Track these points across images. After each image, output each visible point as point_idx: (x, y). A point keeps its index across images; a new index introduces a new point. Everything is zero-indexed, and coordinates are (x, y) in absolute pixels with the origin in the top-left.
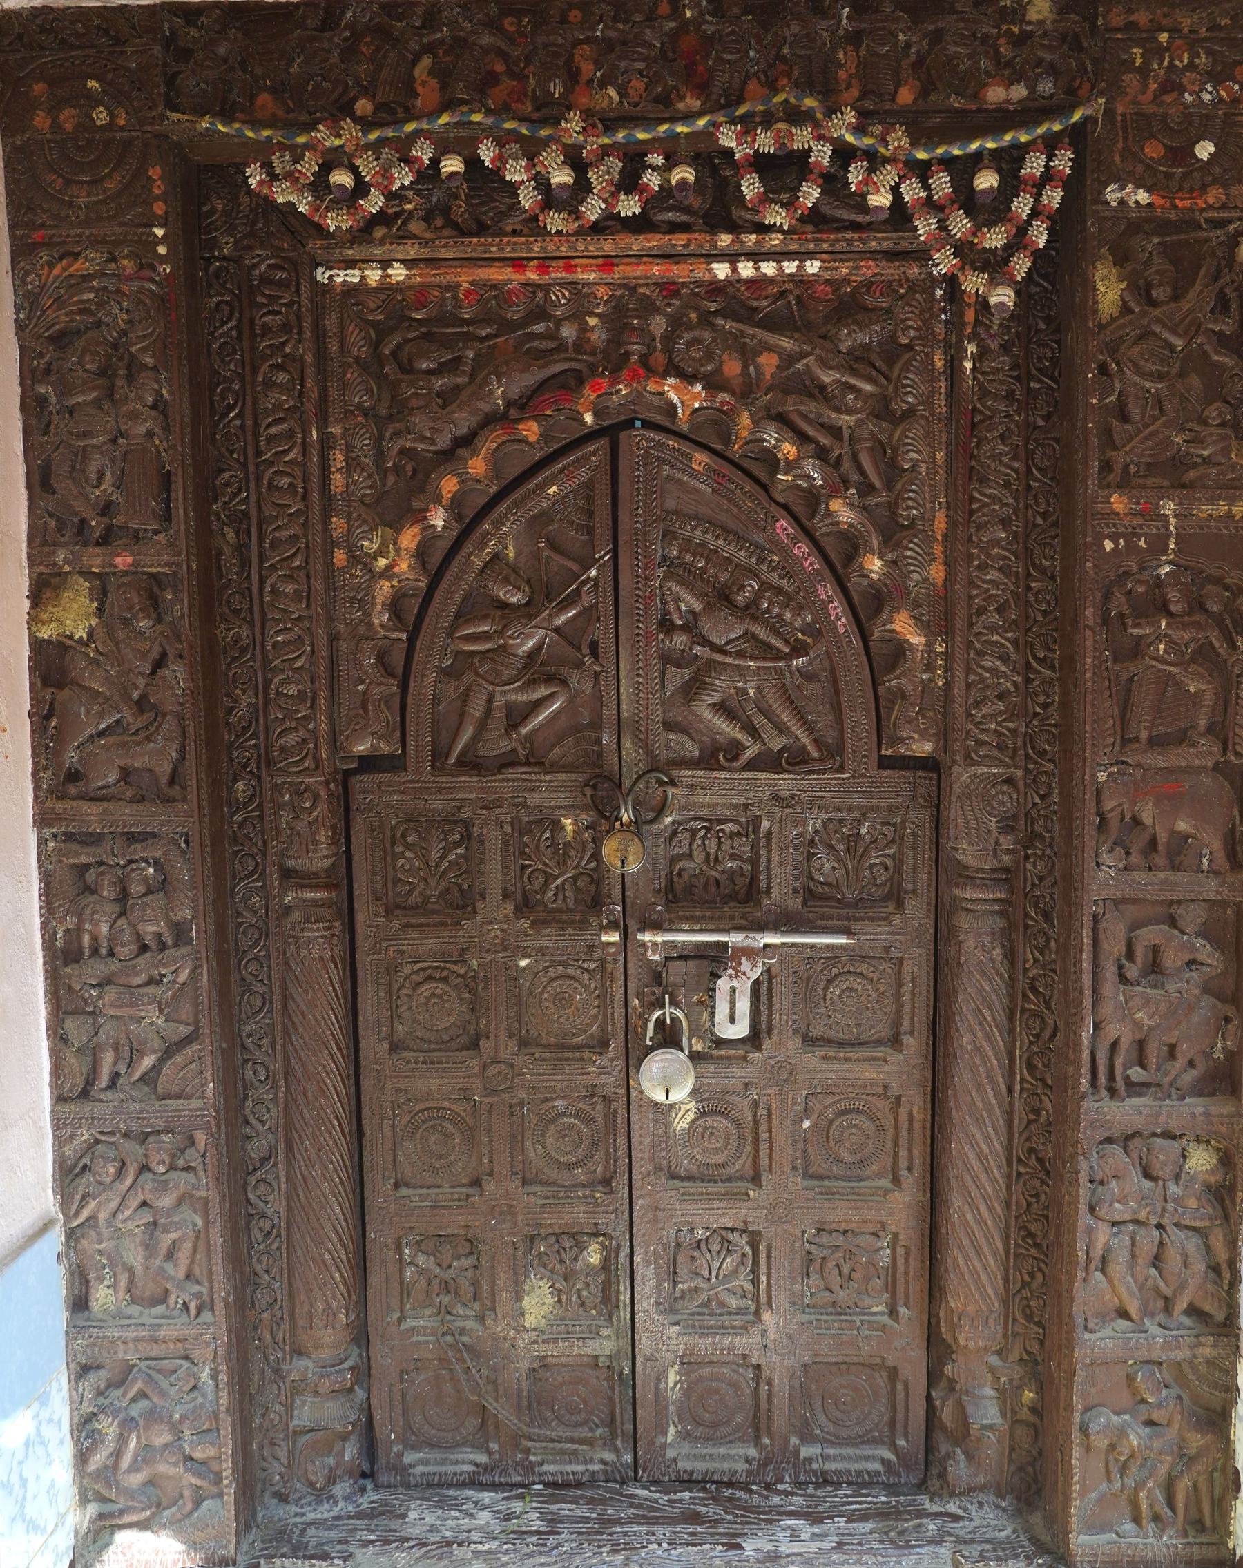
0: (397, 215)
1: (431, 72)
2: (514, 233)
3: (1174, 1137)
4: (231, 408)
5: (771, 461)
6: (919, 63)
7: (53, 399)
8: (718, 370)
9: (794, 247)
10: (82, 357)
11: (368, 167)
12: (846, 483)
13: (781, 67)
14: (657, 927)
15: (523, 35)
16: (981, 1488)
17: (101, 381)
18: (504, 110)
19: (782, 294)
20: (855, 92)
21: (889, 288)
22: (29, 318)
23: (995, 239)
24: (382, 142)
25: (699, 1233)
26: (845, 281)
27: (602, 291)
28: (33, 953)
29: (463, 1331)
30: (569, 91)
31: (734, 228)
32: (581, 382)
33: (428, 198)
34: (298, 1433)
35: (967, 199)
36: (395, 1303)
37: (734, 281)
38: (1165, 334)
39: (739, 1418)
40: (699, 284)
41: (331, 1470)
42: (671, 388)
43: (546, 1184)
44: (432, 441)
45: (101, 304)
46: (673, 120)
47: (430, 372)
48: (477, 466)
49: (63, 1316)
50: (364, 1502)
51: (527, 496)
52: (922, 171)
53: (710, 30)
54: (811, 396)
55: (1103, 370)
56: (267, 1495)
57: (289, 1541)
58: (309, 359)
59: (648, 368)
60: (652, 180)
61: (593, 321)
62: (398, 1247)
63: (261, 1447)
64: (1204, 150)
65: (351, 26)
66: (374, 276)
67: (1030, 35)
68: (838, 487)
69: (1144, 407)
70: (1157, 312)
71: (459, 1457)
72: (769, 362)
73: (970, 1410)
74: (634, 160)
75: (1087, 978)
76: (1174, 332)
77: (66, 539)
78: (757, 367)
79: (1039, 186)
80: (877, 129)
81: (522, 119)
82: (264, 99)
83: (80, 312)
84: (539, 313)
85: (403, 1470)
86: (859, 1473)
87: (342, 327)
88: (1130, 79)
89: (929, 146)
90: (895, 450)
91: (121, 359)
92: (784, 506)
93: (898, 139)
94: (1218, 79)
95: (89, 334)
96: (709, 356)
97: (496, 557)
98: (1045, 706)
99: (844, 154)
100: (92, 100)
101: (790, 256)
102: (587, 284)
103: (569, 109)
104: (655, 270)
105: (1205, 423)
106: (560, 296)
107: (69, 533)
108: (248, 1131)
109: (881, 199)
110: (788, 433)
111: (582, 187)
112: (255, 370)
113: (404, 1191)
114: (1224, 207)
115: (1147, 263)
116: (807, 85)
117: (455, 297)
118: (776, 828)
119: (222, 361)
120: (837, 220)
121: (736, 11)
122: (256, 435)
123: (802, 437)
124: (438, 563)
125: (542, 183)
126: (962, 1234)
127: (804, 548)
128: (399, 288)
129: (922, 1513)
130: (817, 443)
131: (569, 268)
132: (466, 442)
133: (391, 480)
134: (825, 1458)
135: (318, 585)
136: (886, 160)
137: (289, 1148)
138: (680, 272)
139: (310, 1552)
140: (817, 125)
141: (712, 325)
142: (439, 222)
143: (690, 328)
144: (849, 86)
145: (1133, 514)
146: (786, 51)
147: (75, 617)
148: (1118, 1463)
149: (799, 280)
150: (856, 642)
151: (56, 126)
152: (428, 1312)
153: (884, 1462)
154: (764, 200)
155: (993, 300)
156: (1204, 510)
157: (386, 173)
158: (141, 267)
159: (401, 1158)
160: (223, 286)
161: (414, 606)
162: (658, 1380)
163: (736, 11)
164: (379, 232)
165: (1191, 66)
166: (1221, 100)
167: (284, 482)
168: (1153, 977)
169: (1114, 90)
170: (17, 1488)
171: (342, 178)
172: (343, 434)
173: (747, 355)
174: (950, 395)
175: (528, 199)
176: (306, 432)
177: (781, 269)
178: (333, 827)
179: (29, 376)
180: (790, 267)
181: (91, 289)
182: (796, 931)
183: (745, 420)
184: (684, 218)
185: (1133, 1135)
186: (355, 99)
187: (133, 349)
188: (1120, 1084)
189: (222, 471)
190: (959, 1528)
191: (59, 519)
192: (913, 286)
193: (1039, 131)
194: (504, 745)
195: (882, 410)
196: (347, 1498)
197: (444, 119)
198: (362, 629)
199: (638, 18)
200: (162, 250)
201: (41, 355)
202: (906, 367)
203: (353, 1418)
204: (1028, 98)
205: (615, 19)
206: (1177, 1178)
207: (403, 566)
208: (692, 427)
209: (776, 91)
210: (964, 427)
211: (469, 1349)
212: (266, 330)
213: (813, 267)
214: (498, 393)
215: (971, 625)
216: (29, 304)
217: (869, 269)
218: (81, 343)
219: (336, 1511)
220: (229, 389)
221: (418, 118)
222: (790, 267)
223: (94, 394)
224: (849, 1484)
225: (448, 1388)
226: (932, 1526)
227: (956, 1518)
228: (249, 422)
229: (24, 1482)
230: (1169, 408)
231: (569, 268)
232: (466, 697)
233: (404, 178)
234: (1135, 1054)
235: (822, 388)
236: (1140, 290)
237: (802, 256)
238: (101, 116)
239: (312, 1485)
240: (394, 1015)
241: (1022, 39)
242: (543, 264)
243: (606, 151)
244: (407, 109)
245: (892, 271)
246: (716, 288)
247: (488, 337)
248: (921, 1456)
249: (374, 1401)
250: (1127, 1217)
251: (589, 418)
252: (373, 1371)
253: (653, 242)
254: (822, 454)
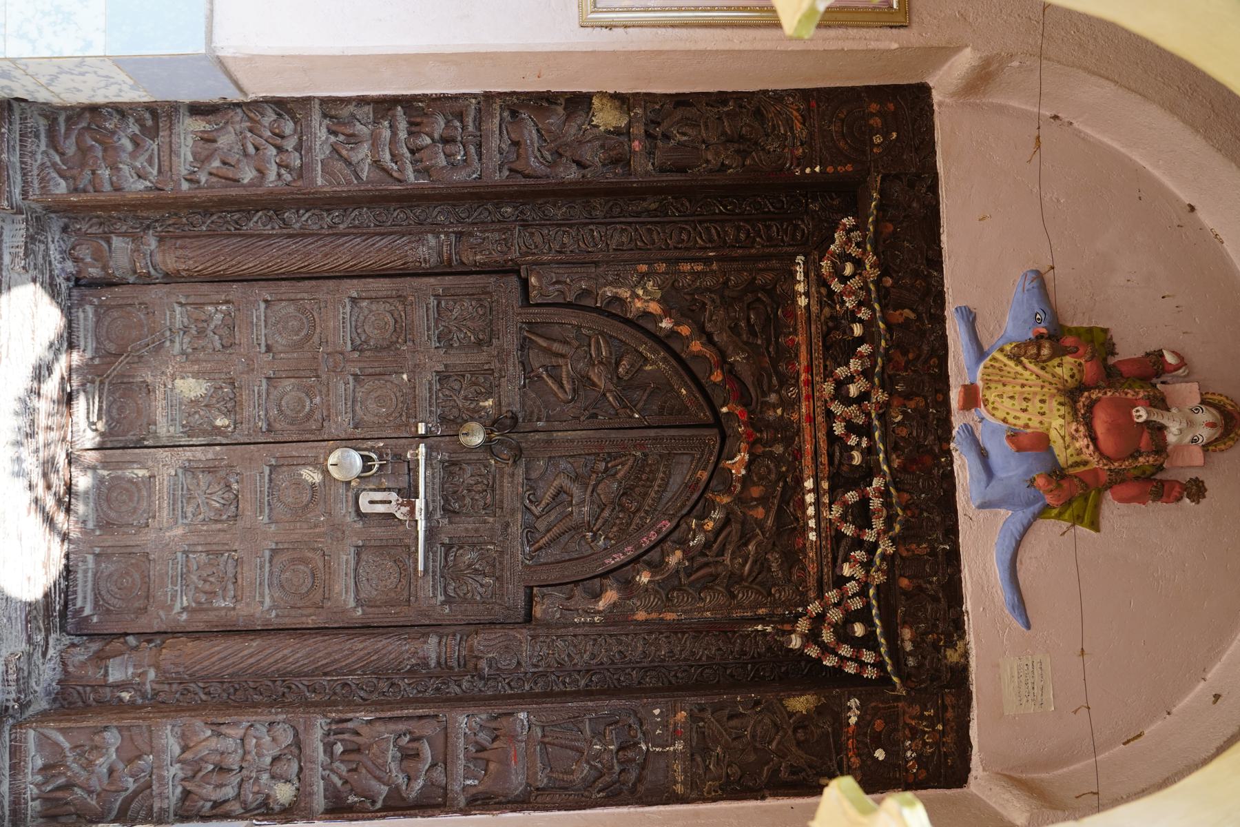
0: (833, 301)
1: (907, 318)
2: (825, 367)
3: (298, 776)
4: (725, 207)
5: (702, 517)
6: (920, 588)
7: (726, 109)
8: (754, 484)
9: (823, 525)
10: (749, 125)
11: (855, 283)
12: (692, 559)
13: (917, 512)
14: (428, 457)
15: (929, 368)
16: (65, 671)
18: (888, 359)
19: (797, 519)
20: (905, 554)
21: (803, 581)
23: (827, 636)
24: (869, 291)
25: (235, 486)
26: (806, 555)
27: (795, 416)
28: (409, 89)
29: (172, 341)
30: (900, 394)
31: (832, 490)
32: (745, 405)
33: (843, 318)
34: (109, 242)
35: (851, 617)
36: (191, 300)
37: (804, 492)
38: (778, 737)
39: (113, 514)
40: (801, 471)
41: (82, 259)
42: (742, 457)
43: (268, 394)
44: (710, 320)
45: (778, 137)
46: (886, 453)
47: (748, 319)
48: (696, 346)
49: (187, 101)
50: (60, 280)
51: (681, 376)
52: (863, 593)
53: (935, 471)
54: (741, 538)
55: (757, 703)
56: (66, 220)
57: (37, 233)
58: (753, 251)
59: (752, 445)
60: (853, 440)
61: (779, 411)
62: (227, 302)
63: (98, 217)
64: (880, 754)
65: (930, 274)
66: (801, 288)
67: (939, 652)
68: (689, 555)
69: (736, 728)
70: (790, 732)
71: (89, 340)
72: (759, 513)
73: (118, 660)
74: (865, 430)
75: (397, 713)
76: (779, 743)
78: (756, 506)
79: (857, 659)
80: (884, 566)
81: (883, 368)
82: (890, 227)
83: (773, 125)
84: (784, 381)
85: (81, 303)
86: (75, 592)
87: (772, 270)
88: (917, 709)
89: (878, 596)
90: (711, 588)
92: (678, 525)
93: (878, 578)
94: (918, 759)
96: (761, 478)
97: (646, 359)
98: (564, 683)
99: (872, 548)
100: (886, 135)
101: (818, 523)
102: (800, 408)
103: (890, 395)
104: (808, 446)
105: (729, 765)
106: (792, 393)
107: (651, 116)
108: (301, 212)
109: (847, 571)
110: (719, 524)
111: (847, 401)
112: (746, 221)
113: (263, 305)
114: (849, 767)
115: (817, 726)
116: (906, 526)
117: (790, 333)
118: (488, 526)
120: (838, 548)
121: (945, 486)
122: (711, 221)
123: (717, 532)
124: (641, 325)
125: (851, 379)
126: (236, 647)
127: (654, 537)
128: (795, 302)
129: (48, 631)
130: (715, 542)
131: (808, 398)
132: (710, 340)
133: (688, 297)
134: (86, 571)
135: (626, 255)
136: (868, 572)
137: (290, 236)
138: (807, 460)
139: (30, 246)
140: (885, 532)
141: (779, 480)
142: (830, 324)
143: (778, 466)
144: (908, 550)
145: (675, 724)
146: (925, 514)
147: (606, 118)
148: (87, 752)
149: (805, 529)
150: (600, 570)
151: (872, 115)
152: (185, 320)
153: (82, 609)
154: (845, 504)
155: (793, 636)
156: (678, 767)
157: (853, 293)
159: (284, 304)
161: (616, 310)
162: (139, 463)
163: (945, 486)
164: (823, 291)
165: (925, 744)
166: (907, 762)
167: (684, 236)
168: (399, 754)
169: (910, 700)
170: (78, 70)
171: (849, 269)
172: (712, 271)
173: (763, 501)
174: (743, 618)
175: (841, 372)
176: (712, 249)
177: (810, 518)
178: (484, 264)
179: (739, 96)
180: (812, 523)
182: (427, 539)
183: (726, 500)
184: (836, 462)
185: (300, 749)
186: (892, 277)
188: (332, 738)
189: (690, 202)
190: (38, 655)
192: (804, 594)
193: (887, 658)
194: (536, 364)
195: (735, 578)
196: (63, 269)
197: (882, 325)
198: (602, 281)
199: (939, 432)
200: (808, 170)
201: (750, 103)
202: (758, 592)
203: (117, 273)
204: (905, 652)
205: (938, 419)
206: (273, 777)
207: (639, 304)
208: (723, 469)
209: (904, 510)
210: (724, 629)
211: (161, 345)
212: (768, 228)
213: (812, 536)
214: (737, 358)
215: (611, 636)
216: (778, 97)
217: (812, 569)
218: (756, 125)
219: (55, 263)
221: (881, 311)
222: (812, 523)
224: (67, 586)
225: (135, 333)
226: (39, 638)
227: (44, 654)
228: (717, 218)
229: (83, 74)
230: (736, 743)
231: (808, 398)
232: (565, 342)
233: (850, 303)
234: (350, 747)
235: (746, 544)
236: (802, 722)
237: (818, 530)
238: (878, 139)
239: (73, 248)
240: (372, 299)
241: (936, 647)
242: (810, 383)
243: (868, 415)
244: (887, 305)
245: (812, 582)
246: (799, 481)
247: (769, 353)
248: (85, 632)
249: (125, 288)
250: (247, 747)
251: (725, 410)
252: (145, 287)
253: (823, 445)
254: (707, 545)
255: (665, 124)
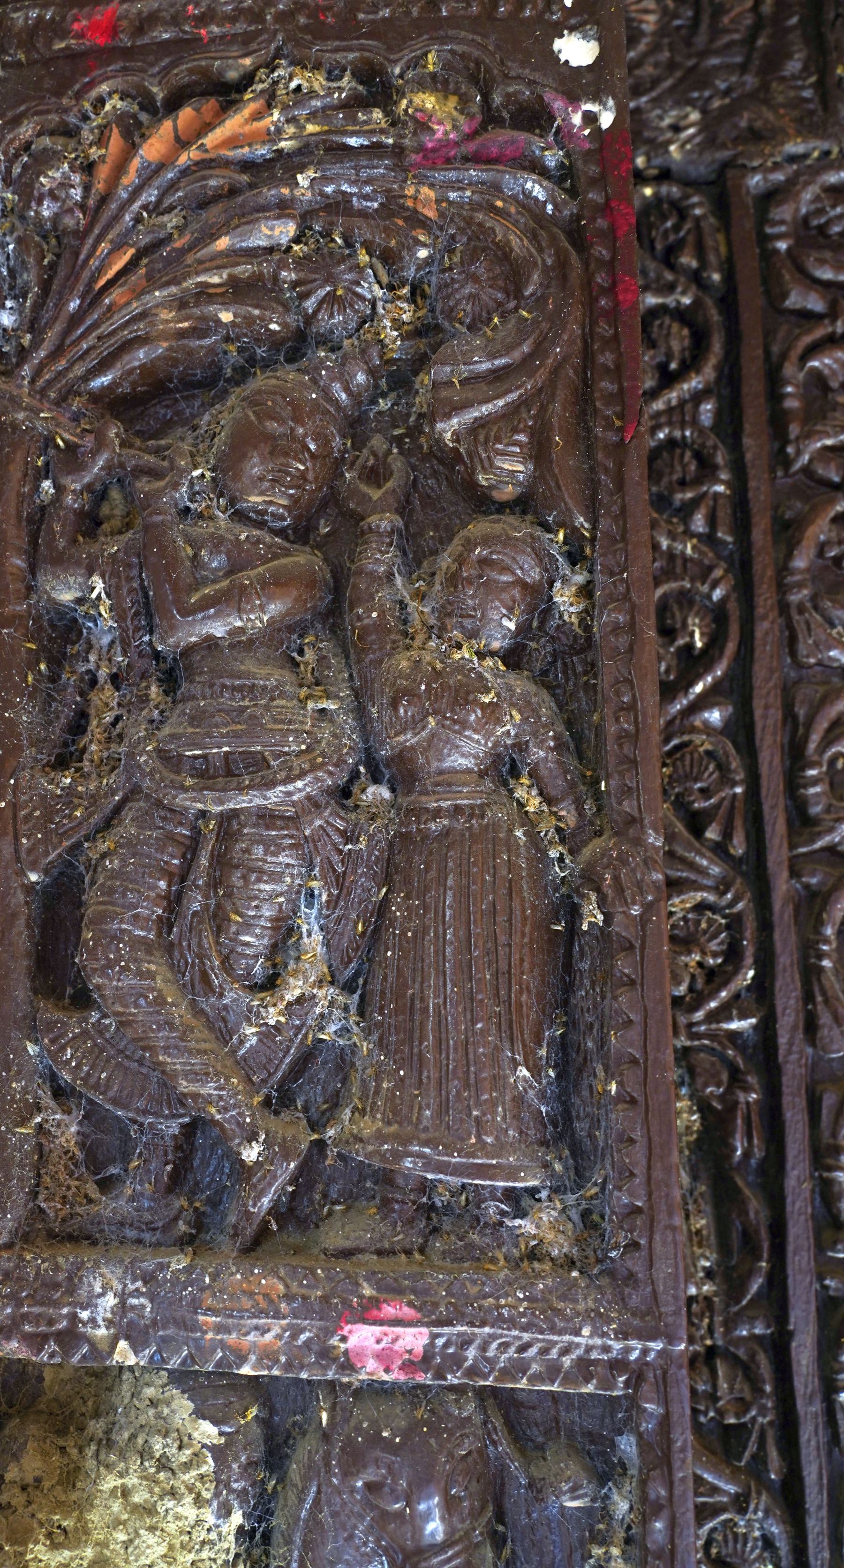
7: (105, 626)
10: (227, 468)
17: (303, 558)
22: (33, 324)
45: (320, 264)
77: (114, 1206)
83: (237, 291)
91: (375, 475)
95: (260, 381)
107: (134, 1195)
119: (661, 502)
158: (490, 118)
160: (669, 258)
181: (283, 209)
187: (449, 428)
191: (93, 1116)
201: (72, 458)
218: (225, 416)
220: (685, 599)
223: (275, 608)
255: (220, 1096)
